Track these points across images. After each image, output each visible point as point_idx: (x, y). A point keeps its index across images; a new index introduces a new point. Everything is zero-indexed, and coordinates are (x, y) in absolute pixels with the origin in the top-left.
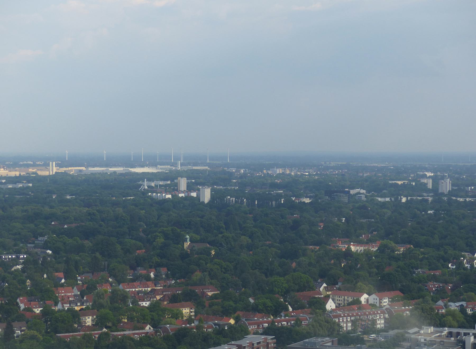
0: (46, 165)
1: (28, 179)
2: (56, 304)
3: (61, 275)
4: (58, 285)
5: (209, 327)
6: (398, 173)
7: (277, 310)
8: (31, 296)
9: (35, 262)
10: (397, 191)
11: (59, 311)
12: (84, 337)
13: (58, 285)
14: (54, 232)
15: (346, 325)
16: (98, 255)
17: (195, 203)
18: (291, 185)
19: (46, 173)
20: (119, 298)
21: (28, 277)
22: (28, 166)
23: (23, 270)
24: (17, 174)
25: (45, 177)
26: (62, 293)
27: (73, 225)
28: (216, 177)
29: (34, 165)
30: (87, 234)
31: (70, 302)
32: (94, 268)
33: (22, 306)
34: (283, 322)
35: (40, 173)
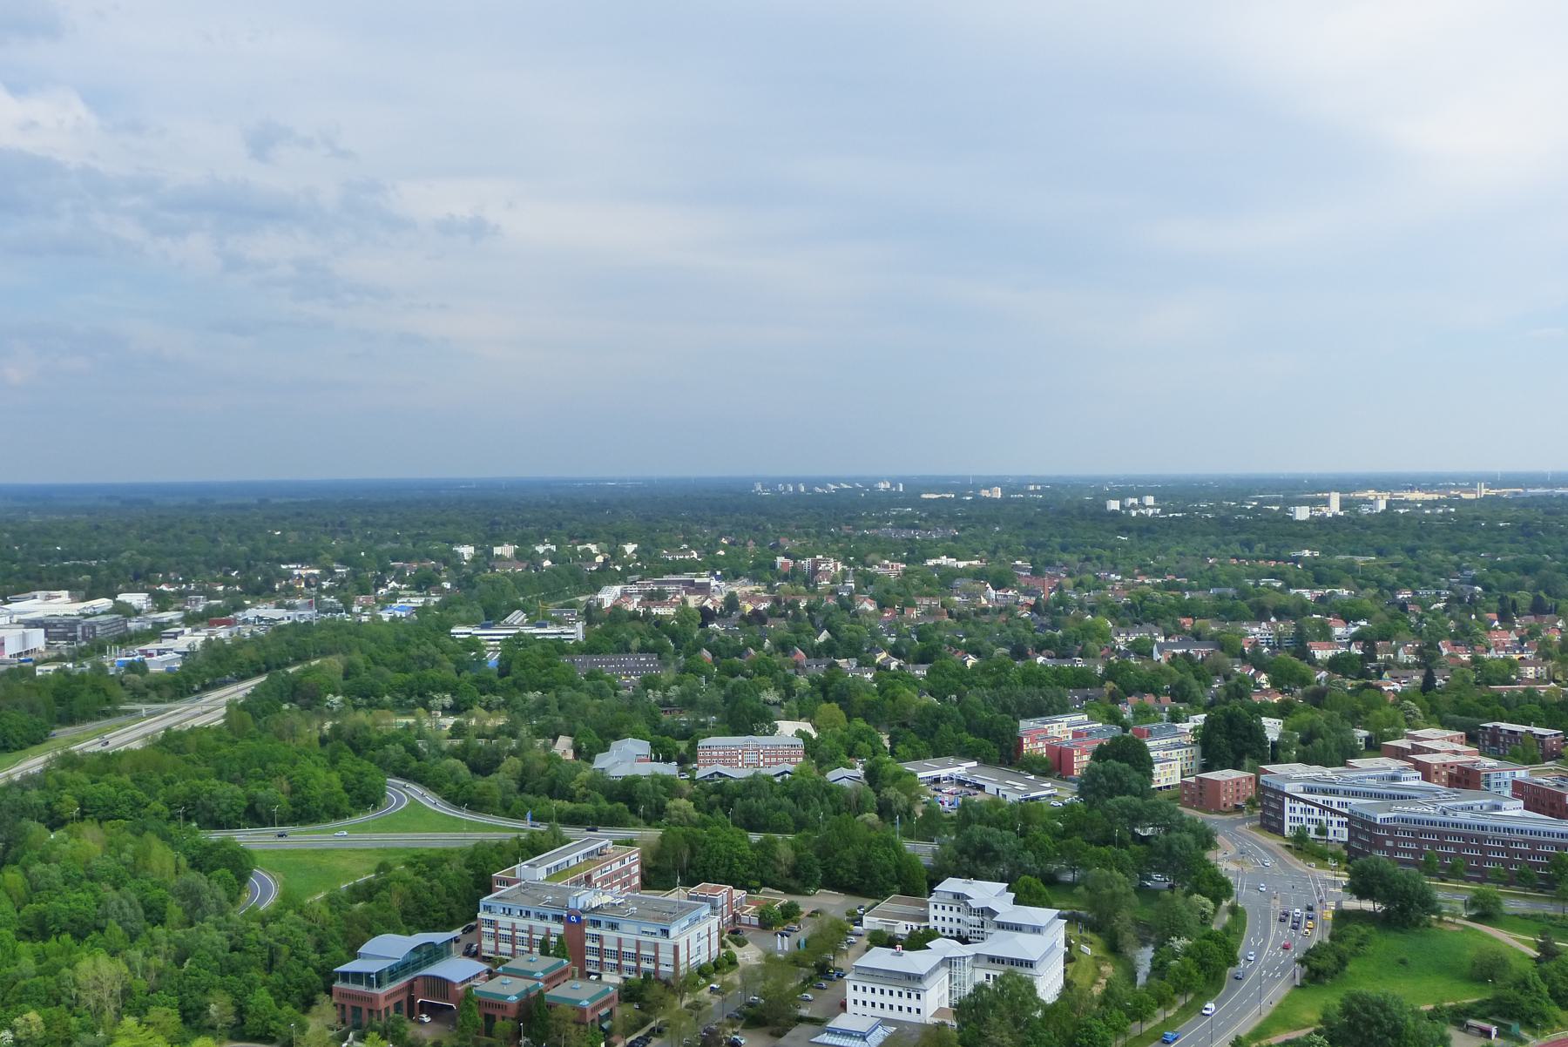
0: (1472, 487)
1: (1450, 503)
2: (1488, 650)
3: (1494, 616)
4: (1488, 628)
9: (1460, 600)
11: (1492, 659)
12: (1525, 690)
13: (1488, 628)
14: (1483, 565)
16: (1542, 593)
19: (1472, 496)
21: (1452, 618)
22: (1450, 487)
23: (1446, 610)
24: (1436, 497)
25: (1471, 501)
26: (1496, 637)
27: (1510, 558)
29: (1456, 488)
30: (1527, 569)
31: (1507, 650)
32: (1538, 609)
33: (1445, 652)
35: (1464, 496)
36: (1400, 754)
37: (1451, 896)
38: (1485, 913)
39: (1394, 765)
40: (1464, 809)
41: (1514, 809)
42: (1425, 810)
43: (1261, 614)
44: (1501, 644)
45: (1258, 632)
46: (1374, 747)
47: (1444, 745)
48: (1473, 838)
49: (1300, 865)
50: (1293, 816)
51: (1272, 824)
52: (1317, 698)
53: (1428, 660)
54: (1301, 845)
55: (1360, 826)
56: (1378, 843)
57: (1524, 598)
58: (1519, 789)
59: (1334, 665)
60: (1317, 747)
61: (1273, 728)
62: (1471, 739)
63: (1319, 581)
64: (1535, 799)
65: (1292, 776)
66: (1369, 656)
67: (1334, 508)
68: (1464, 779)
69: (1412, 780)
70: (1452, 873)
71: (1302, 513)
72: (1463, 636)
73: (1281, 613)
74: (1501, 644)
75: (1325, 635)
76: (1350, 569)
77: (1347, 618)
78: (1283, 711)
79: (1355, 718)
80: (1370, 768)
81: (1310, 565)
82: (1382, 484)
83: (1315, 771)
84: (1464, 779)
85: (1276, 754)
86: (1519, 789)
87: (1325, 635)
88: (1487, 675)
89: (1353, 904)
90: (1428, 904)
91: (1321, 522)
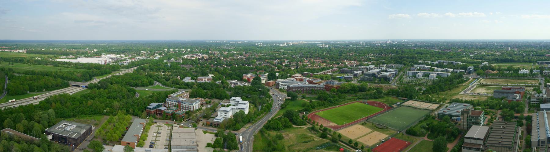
5: (328, 67)
6: (357, 42)
7: (339, 64)
8: (300, 62)
10: (357, 45)
15: (349, 66)
17: (326, 48)
18: (340, 45)
20: (314, 62)
28: (329, 43)
30: (309, 52)
32: (310, 57)
34: (340, 66)
36: (293, 77)
37: (300, 96)
38: (304, 98)
39: (293, 79)
40: (301, 84)
41: (307, 83)
42: (296, 85)
43: (276, 59)
44: (306, 62)
45: (276, 61)
46: (290, 76)
47: (299, 76)
48: (302, 88)
49: (280, 93)
50: (280, 86)
51: (277, 88)
52: (283, 70)
53: (297, 64)
54: (281, 90)
55: (288, 87)
56: (291, 89)
57: (309, 56)
58: (308, 81)
59: (285, 66)
60: (283, 77)
61: (277, 74)
62: (302, 75)
63: (284, 54)
64: (310, 82)
65: (280, 81)
66: (290, 64)
67: (286, 45)
68: (301, 80)
69: (295, 81)
70: (300, 93)
71: (281, 45)
72: (301, 61)
73: (279, 59)
74: (306, 62)
75: (284, 62)
76: (287, 53)
77: (287, 59)
78: (279, 72)
79: (288, 73)
80: (290, 79)
81: (282, 52)
82: (292, 42)
83: (283, 80)
84: (301, 80)
85: (278, 78)
86: (308, 81)
87: (284, 62)
88: (304, 66)
89: (287, 98)
90: (297, 97)
91: (284, 46)
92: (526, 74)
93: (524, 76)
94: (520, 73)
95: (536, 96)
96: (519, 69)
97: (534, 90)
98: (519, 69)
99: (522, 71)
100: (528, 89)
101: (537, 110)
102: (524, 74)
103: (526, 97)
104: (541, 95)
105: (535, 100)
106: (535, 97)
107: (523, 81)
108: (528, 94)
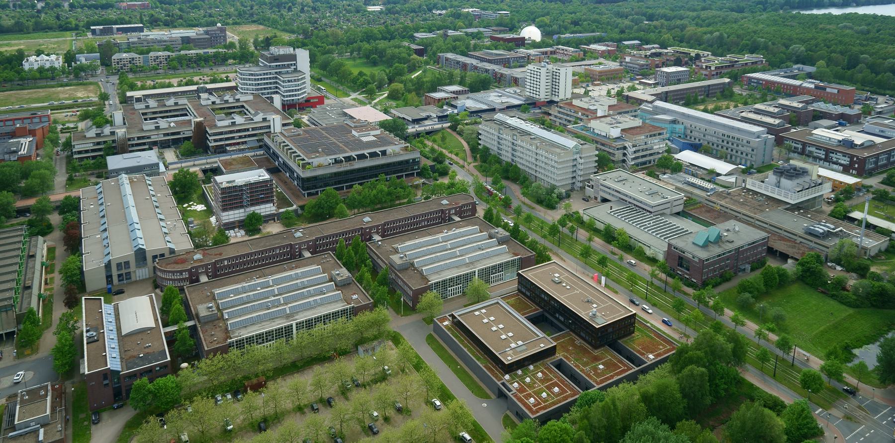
92: (52, 69)
93: (46, 76)
94: (26, 66)
95: (92, 133)
96: (20, 56)
97: (84, 117)
98: (20, 56)
99: (32, 63)
100: (61, 115)
101: (99, 176)
102: (41, 70)
103: (55, 142)
104: (107, 130)
105: (90, 146)
106: (88, 136)
107: (42, 93)
108: (62, 131)
